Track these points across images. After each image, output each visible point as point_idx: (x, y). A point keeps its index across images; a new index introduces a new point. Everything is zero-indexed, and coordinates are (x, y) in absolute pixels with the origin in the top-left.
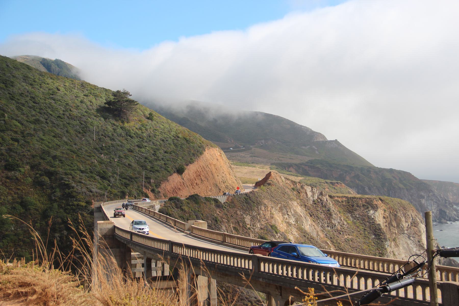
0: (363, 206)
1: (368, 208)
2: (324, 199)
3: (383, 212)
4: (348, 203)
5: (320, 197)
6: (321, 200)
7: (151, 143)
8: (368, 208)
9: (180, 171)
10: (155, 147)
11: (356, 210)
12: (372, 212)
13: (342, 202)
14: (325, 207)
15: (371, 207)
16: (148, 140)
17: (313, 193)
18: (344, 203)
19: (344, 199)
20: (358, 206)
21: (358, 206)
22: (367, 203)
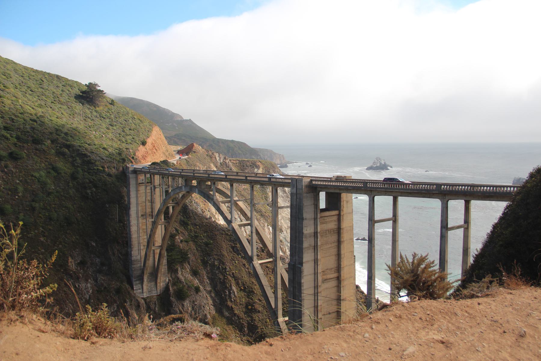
0: (250, 166)
1: (253, 167)
2: (227, 161)
3: (262, 170)
4: (240, 164)
5: (224, 160)
6: (225, 162)
7: (119, 123)
8: (253, 167)
9: (144, 143)
10: (122, 125)
11: (246, 169)
12: (256, 170)
13: (236, 163)
14: (228, 167)
15: (256, 166)
16: (116, 121)
17: (220, 158)
18: (238, 165)
19: (237, 162)
20: (247, 166)
21: (247, 166)
22: (253, 164)
